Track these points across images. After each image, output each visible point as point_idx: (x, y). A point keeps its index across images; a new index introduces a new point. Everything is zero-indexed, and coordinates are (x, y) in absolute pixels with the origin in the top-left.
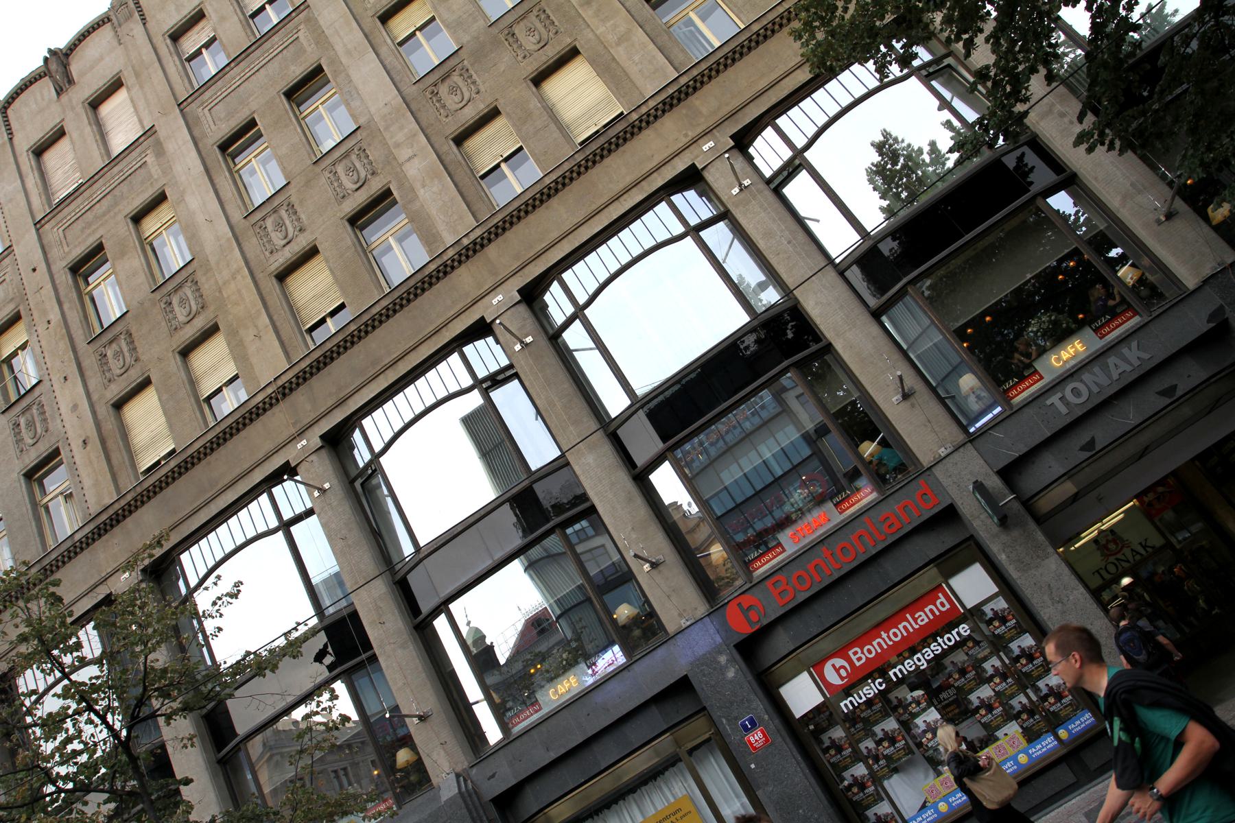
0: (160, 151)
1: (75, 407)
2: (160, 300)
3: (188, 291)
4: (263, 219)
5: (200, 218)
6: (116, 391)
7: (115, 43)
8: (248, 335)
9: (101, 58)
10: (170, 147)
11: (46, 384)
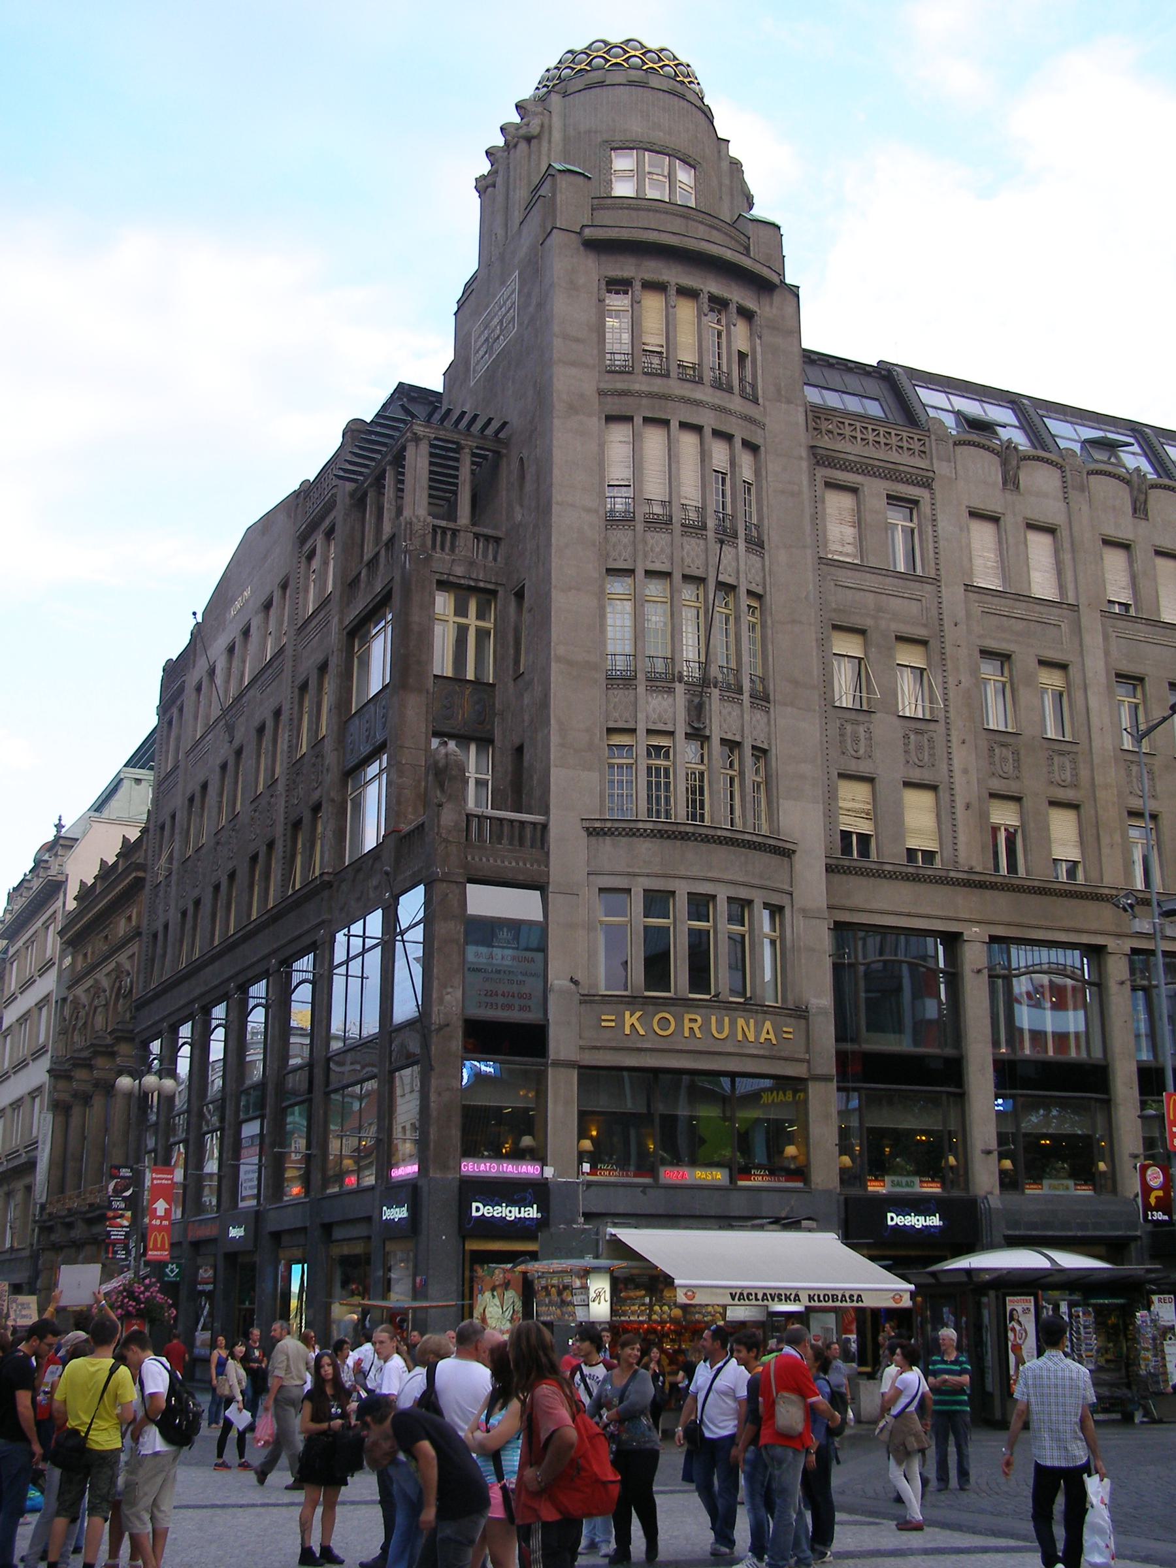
0: (1077, 629)
1: (965, 771)
2: (1048, 749)
3: (1066, 761)
4: (1132, 762)
5: (1094, 720)
6: (996, 785)
7: (1061, 495)
8: (1105, 840)
10: (1087, 639)
11: (940, 728)
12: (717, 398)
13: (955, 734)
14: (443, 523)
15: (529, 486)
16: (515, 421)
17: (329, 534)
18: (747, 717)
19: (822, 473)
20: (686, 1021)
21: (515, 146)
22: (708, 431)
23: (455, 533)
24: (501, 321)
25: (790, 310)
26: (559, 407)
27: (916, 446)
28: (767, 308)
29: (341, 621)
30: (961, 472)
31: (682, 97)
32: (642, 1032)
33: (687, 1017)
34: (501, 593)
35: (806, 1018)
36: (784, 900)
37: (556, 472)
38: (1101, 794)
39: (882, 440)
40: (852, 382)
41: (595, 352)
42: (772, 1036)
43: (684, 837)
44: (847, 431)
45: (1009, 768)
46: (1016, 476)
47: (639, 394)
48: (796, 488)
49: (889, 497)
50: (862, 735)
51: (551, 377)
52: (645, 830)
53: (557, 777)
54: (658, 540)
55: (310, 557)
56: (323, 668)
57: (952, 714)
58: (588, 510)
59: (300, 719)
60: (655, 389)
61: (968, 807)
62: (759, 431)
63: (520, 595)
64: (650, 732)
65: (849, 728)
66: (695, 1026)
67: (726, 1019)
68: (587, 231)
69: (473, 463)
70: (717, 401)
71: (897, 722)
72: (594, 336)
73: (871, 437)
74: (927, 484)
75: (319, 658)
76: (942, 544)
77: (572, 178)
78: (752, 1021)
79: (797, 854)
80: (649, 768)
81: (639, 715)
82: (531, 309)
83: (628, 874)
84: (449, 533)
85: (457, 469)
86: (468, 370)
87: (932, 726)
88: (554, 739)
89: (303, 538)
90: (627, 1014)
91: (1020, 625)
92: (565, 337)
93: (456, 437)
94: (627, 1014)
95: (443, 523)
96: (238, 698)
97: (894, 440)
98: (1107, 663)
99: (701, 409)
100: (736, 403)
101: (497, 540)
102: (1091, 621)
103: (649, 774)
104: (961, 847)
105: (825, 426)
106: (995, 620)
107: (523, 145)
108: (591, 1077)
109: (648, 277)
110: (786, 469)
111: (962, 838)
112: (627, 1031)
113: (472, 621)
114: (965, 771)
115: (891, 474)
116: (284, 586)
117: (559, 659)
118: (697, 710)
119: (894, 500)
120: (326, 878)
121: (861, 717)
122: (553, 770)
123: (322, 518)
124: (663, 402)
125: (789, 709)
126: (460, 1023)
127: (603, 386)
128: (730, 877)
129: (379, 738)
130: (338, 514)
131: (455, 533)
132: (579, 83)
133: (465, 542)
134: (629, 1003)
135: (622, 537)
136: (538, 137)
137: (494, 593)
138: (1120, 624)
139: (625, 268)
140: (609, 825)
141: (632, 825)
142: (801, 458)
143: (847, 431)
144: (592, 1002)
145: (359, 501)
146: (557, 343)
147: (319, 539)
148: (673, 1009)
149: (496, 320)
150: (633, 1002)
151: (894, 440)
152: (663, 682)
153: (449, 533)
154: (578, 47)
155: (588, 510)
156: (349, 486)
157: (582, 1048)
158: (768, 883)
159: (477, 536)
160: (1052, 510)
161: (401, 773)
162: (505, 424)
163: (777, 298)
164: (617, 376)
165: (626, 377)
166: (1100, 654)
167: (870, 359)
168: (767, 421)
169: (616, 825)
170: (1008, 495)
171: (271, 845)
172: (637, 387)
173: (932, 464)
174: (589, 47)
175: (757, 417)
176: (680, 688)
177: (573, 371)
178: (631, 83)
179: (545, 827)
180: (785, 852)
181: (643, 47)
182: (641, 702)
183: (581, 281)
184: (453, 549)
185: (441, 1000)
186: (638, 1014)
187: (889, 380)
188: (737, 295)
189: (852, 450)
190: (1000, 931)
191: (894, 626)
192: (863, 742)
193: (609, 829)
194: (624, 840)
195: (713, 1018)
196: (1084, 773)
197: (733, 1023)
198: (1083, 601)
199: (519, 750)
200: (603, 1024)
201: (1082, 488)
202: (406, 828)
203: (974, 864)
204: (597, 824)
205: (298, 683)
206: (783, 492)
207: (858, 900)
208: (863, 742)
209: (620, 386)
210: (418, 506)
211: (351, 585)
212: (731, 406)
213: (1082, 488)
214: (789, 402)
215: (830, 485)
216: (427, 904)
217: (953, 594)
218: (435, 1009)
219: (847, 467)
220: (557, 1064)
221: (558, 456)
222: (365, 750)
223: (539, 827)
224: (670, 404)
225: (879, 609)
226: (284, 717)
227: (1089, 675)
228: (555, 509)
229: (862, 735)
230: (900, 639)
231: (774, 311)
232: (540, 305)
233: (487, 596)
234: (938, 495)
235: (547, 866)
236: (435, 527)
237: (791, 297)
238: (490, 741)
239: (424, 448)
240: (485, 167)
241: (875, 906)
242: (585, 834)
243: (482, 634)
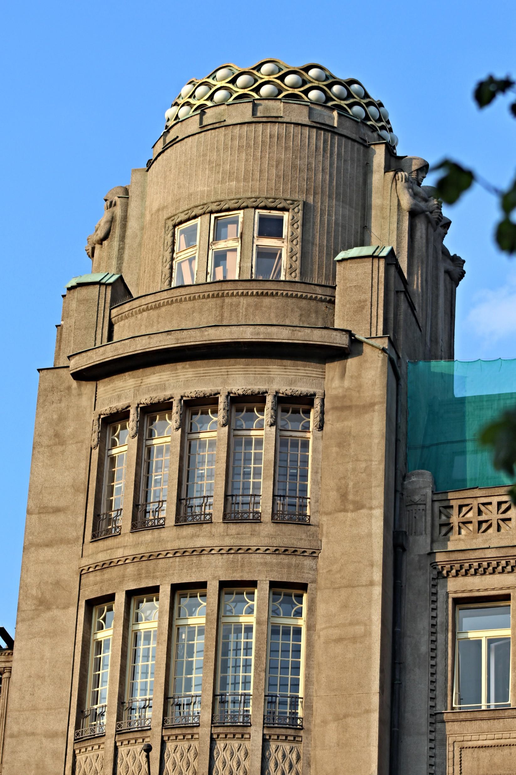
28: (336, 383)
47: (124, 562)
48: (359, 629)
58: (52, 735)
60: (142, 550)
62: (308, 562)
70: (228, 542)
99: (204, 558)
100: (266, 533)
124: (151, 564)
155: (52, 735)
172: (119, 553)
175: (303, 544)
188: (280, 379)
206: (340, 640)
224: (162, 563)
231: (347, 383)
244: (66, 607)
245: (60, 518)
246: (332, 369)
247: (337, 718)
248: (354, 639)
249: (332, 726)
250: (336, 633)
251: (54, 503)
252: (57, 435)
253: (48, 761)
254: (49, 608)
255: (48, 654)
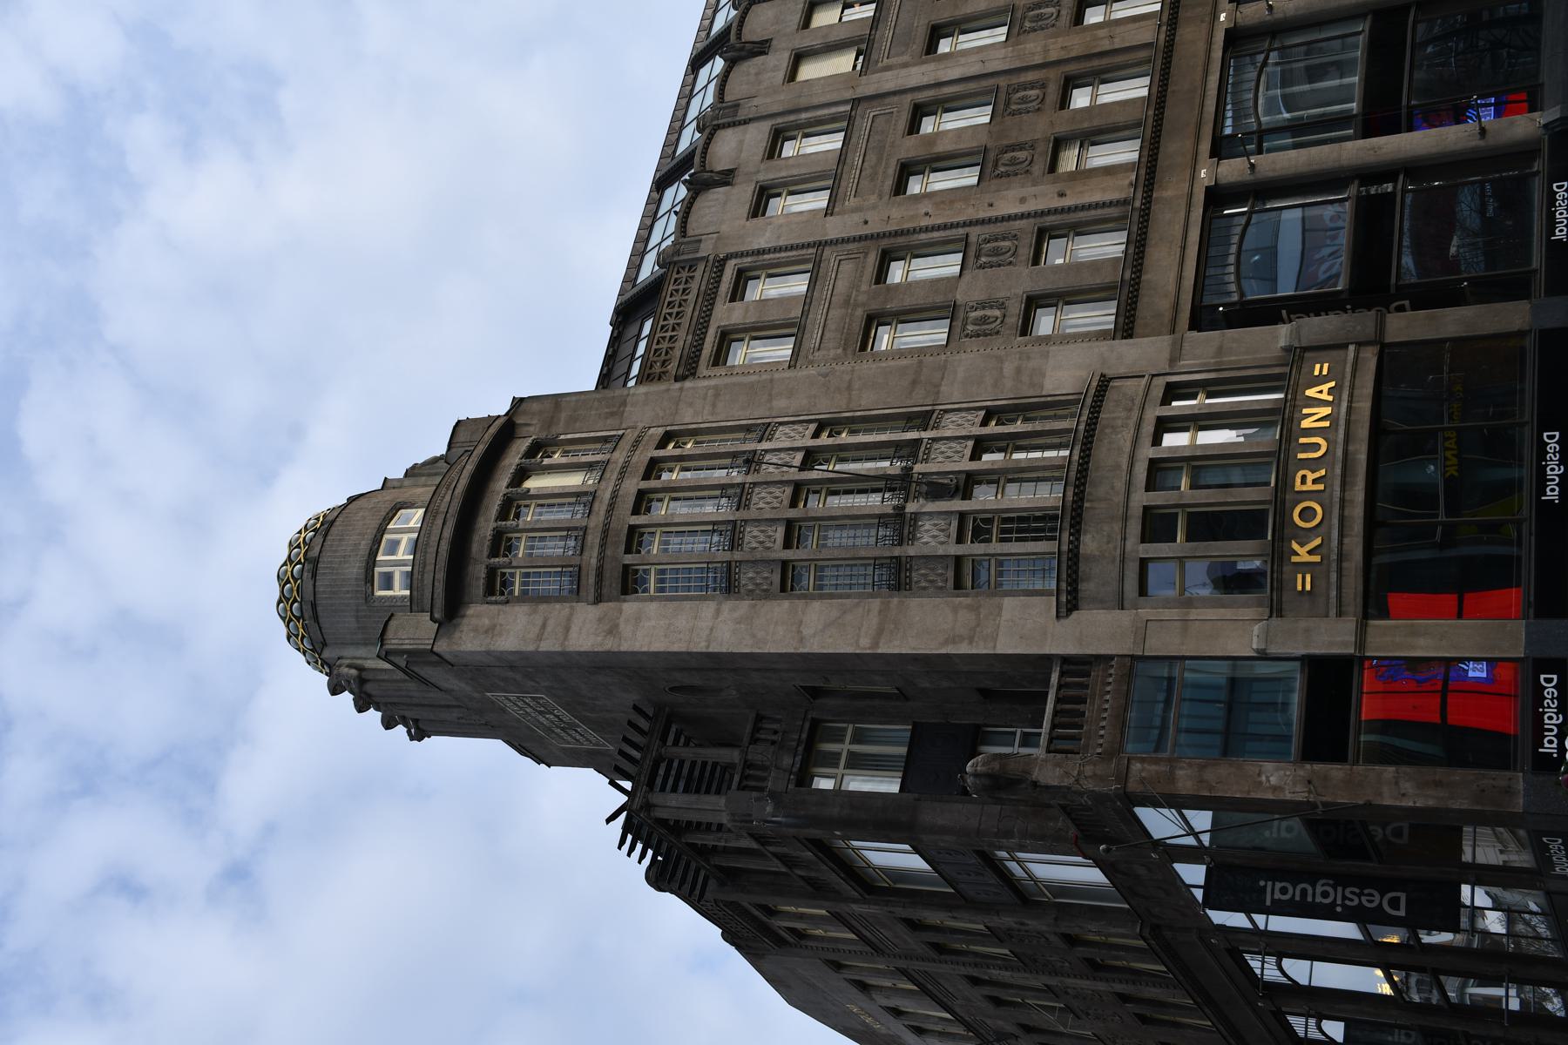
6: (1039, 168)
8: (1106, 45)
9: (741, 142)
10: (889, 86)
12: (612, 476)
13: (982, 215)
14: (737, 778)
15: (696, 681)
16: (633, 697)
17: (772, 912)
18: (948, 433)
19: (703, 369)
20: (1304, 488)
21: (369, 696)
22: (645, 485)
23: (748, 765)
24: (541, 713)
25: (535, 406)
26: (609, 645)
27: (684, 274)
29: (855, 901)
30: (711, 229)
31: (333, 521)
32: (1318, 541)
33: (1298, 486)
34: (812, 714)
35: (1305, 349)
36: (1160, 382)
37: (675, 648)
38: (1054, 56)
39: (676, 310)
40: (625, 349)
41: (558, 606)
42: (1325, 387)
43: (1080, 497)
44: (665, 345)
45: (1022, 155)
46: (720, 173)
47: (602, 558)
48: (710, 392)
49: (733, 300)
50: (979, 313)
51: (580, 653)
52: (1070, 542)
53: (1007, 645)
54: (752, 535)
55: (801, 935)
56: (914, 925)
57: (961, 219)
59: (976, 954)
61: (1062, 195)
63: (815, 693)
64: (960, 540)
65: (970, 327)
66: (1311, 476)
67: (1302, 440)
68: (437, 616)
69: (686, 744)
71: (967, 276)
72: (542, 607)
73: (672, 321)
74: (721, 263)
75: (901, 929)
76: (782, 243)
77: (390, 634)
78: (1305, 411)
79: (1106, 372)
80: (1002, 540)
81: (940, 552)
82: (518, 677)
83: (1123, 561)
84: (748, 772)
85: (693, 763)
86: (598, 752)
87: (973, 239)
88: (964, 649)
89: (780, 942)
90: (1295, 559)
91: (872, 158)
92: (540, 638)
93: (648, 763)
94: (1295, 559)
95: (737, 778)
96: (968, 1027)
97: (677, 298)
98: (915, 65)
100: (619, 457)
101: (759, 718)
102: (869, 86)
103: (1009, 540)
104: (1108, 197)
105: (657, 368)
106: (865, 183)
107: (368, 687)
108: (1374, 605)
109: (486, 553)
110: (696, 401)
111: (1097, 197)
112: (1317, 559)
113: (845, 748)
114: (1023, 200)
115: (709, 298)
116: (838, 966)
117: (876, 644)
118: (937, 489)
119: (737, 293)
120: (1146, 933)
121: (961, 315)
122: (999, 651)
123: (754, 918)
125: (943, 388)
126: (1308, 766)
127: (591, 598)
128: (1128, 444)
129: (974, 860)
130: (745, 900)
131: (748, 765)
132: (314, 628)
133: (759, 754)
134: (1281, 559)
135: (747, 577)
136: (361, 669)
137: (815, 724)
138: (874, 56)
139: (477, 574)
140: (1064, 585)
141: (1064, 558)
142: (681, 389)
143: (665, 345)
144: (1280, 601)
145: (730, 876)
146: (545, 646)
147: (779, 924)
148: (1288, 505)
149: (541, 719)
150: (1279, 554)
151: (677, 298)
152: (901, 525)
153: (748, 772)
154: (284, 631)
156: (712, 884)
157: (1340, 614)
158: (1138, 401)
159: (754, 740)
160: (757, 135)
161: (1008, 834)
162: (635, 708)
163: (519, 421)
164: (583, 582)
165: (583, 573)
166: (903, 72)
167: (607, 331)
168: (640, 425)
169: (1064, 576)
170: (738, 180)
171: (1124, 998)
172: (594, 561)
173: (702, 258)
174: (283, 619)
176: (911, 507)
177: (574, 629)
178: (314, 576)
179: (1066, 660)
180: (1104, 383)
181: (285, 564)
182: (926, 551)
183: (487, 621)
184: (764, 768)
185: (1275, 789)
186: (1295, 546)
187: (628, 313)
189: (683, 338)
190: (1205, 146)
191: (864, 287)
192: (988, 312)
193: (1069, 584)
194: (1082, 567)
195: (1301, 456)
196: (1030, 76)
197: (1309, 432)
198: (848, 95)
199: (986, 694)
200: (1308, 587)
201: (736, 106)
202: (1072, 831)
203: (1127, 182)
204: (1064, 598)
205: (933, 954)
206: (714, 405)
207: (1165, 305)
208: (988, 312)
209: (592, 580)
210: (713, 807)
211: (817, 890)
212: (621, 460)
213: (736, 106)
214: (624, 404)
215: (720, 357)
216: (1155, 804)
217: (835, 228)
218: (1288, 796)
219: (698, 347)
220: (1361, 642)
221: (658, 646)
222: (992, 878)
223: (1066, 667)
225: (847, 302)
226: (975, 972)
227: (925, 80)
228: (714, 648)
229: (979, 313)
230: (878, 281)
232: (512, 667)
233: (816, 731)
234: (733, 250)
235: (1111, 657)
236: (741, 788)
237: (524, 406)
238: (978, 727)
239: (657, 798)
240: (400, 730)
241: (1172, 288)
242: (1075, 614)
243: (858, 738)
244: (620, 611)
245: (551, 623)
246: (523, 431)
247: (770, 400)
248: (717, 395)
249: (775, 403)
250: (708, 408)
251: (537, 630)
252: (486, 632)
253: (736, 615)
254: (617, 626)
255: (653, 623)
